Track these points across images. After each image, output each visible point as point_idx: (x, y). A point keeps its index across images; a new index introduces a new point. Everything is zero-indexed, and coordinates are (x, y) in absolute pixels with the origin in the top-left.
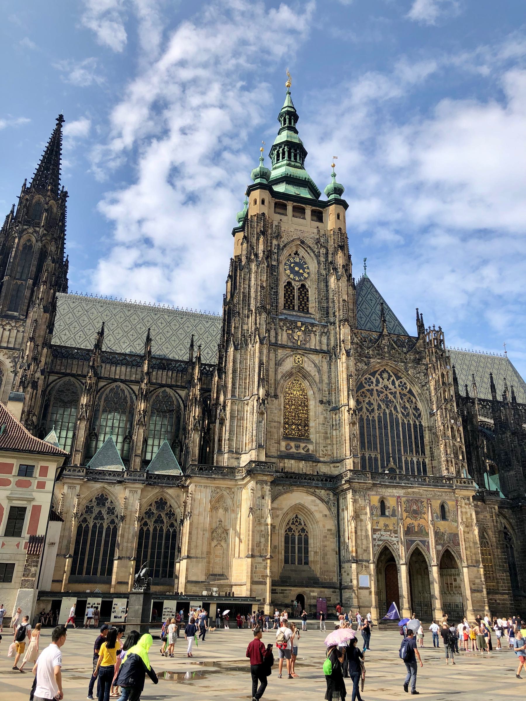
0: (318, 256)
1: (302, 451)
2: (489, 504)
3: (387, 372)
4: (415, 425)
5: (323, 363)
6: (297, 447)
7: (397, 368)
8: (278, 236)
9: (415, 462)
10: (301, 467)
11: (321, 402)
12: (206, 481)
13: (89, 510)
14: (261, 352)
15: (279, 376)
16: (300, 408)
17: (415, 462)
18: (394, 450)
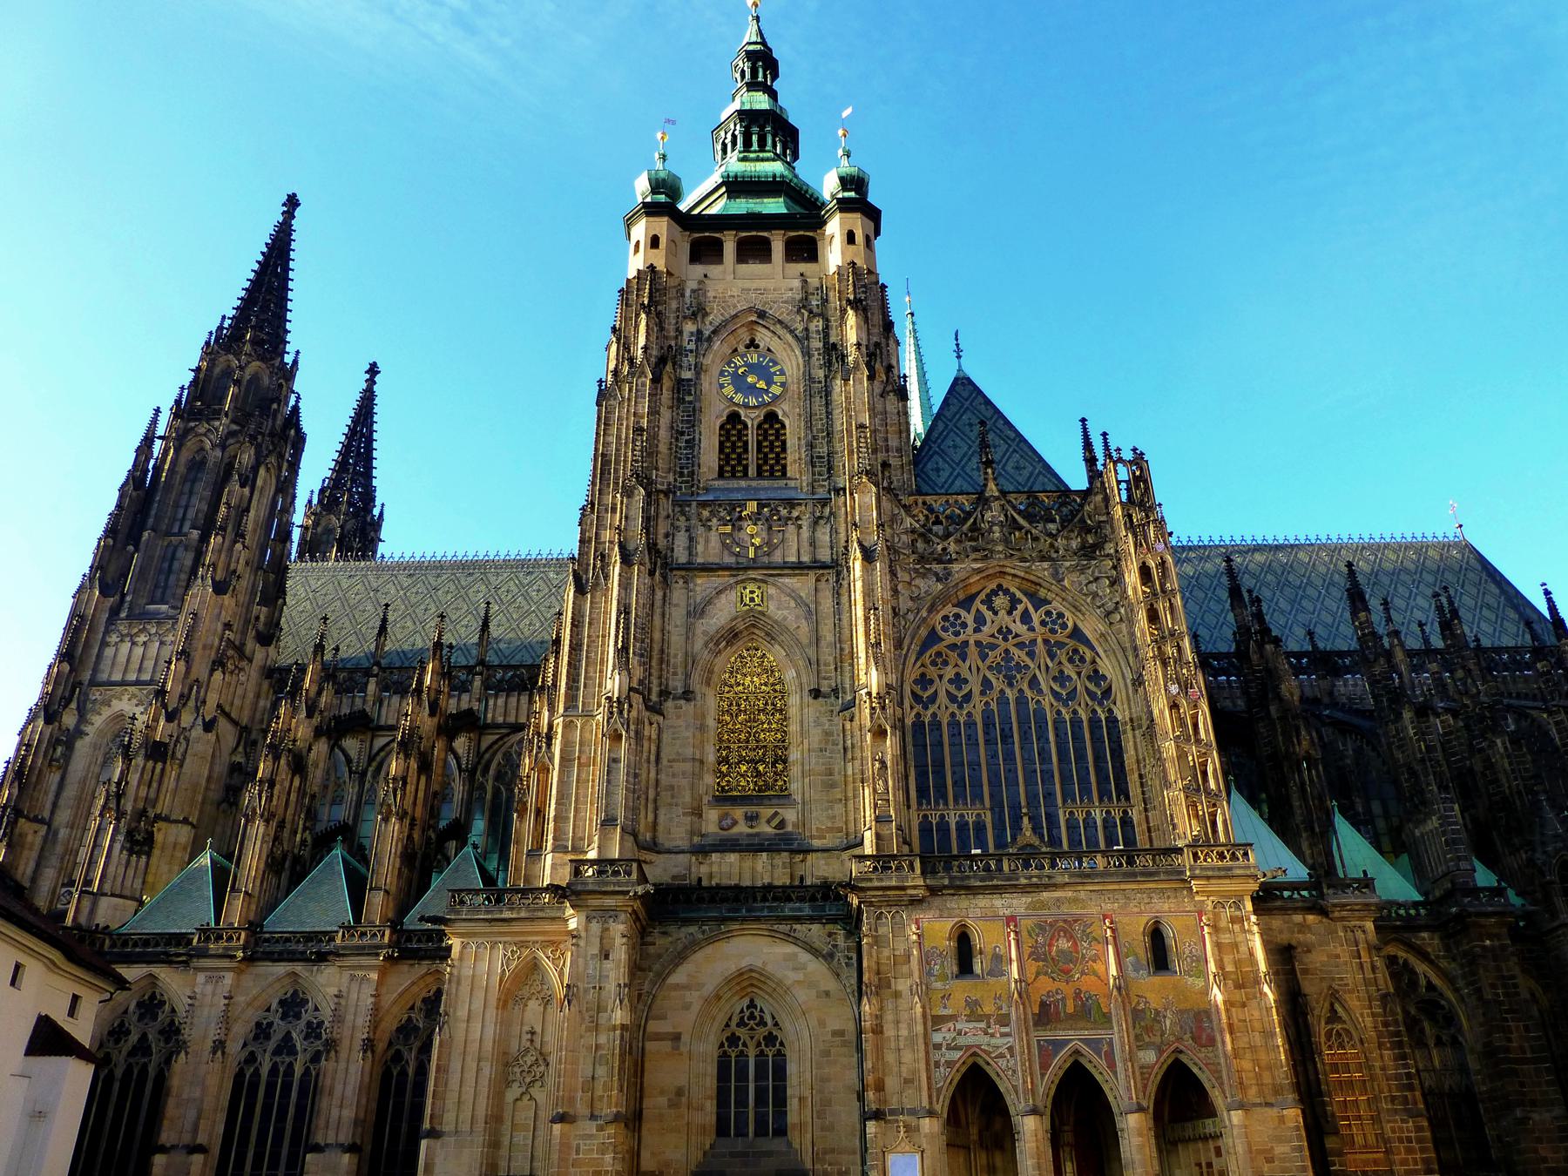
0: (803, 339)
1: (768, 830)
2: (1343, 919)
3: (1006, 592)
4: (1094, 722)
5: (820, 594)
6: (751, 819)
7: (1032, 578)
8: (699, 312)
9: (1099, 822)
10: (765, 870)
11: (816, 693)
12: (488, 930)
13: (262, 1031)
14: (625, 585)
15: (699, 643)
16: (762, 717)
17: (1099, 822)
18: (1032, 799)
